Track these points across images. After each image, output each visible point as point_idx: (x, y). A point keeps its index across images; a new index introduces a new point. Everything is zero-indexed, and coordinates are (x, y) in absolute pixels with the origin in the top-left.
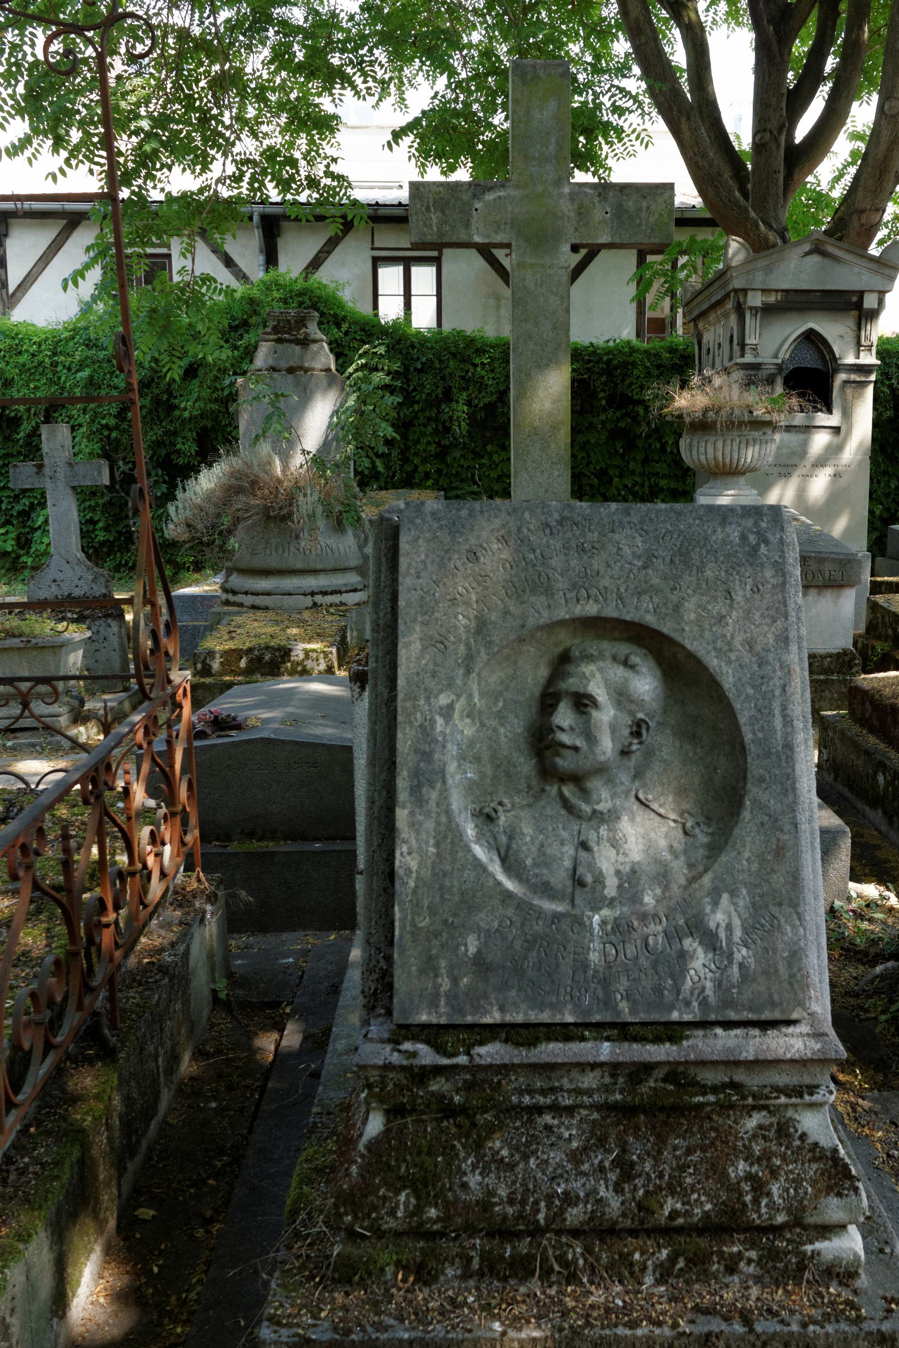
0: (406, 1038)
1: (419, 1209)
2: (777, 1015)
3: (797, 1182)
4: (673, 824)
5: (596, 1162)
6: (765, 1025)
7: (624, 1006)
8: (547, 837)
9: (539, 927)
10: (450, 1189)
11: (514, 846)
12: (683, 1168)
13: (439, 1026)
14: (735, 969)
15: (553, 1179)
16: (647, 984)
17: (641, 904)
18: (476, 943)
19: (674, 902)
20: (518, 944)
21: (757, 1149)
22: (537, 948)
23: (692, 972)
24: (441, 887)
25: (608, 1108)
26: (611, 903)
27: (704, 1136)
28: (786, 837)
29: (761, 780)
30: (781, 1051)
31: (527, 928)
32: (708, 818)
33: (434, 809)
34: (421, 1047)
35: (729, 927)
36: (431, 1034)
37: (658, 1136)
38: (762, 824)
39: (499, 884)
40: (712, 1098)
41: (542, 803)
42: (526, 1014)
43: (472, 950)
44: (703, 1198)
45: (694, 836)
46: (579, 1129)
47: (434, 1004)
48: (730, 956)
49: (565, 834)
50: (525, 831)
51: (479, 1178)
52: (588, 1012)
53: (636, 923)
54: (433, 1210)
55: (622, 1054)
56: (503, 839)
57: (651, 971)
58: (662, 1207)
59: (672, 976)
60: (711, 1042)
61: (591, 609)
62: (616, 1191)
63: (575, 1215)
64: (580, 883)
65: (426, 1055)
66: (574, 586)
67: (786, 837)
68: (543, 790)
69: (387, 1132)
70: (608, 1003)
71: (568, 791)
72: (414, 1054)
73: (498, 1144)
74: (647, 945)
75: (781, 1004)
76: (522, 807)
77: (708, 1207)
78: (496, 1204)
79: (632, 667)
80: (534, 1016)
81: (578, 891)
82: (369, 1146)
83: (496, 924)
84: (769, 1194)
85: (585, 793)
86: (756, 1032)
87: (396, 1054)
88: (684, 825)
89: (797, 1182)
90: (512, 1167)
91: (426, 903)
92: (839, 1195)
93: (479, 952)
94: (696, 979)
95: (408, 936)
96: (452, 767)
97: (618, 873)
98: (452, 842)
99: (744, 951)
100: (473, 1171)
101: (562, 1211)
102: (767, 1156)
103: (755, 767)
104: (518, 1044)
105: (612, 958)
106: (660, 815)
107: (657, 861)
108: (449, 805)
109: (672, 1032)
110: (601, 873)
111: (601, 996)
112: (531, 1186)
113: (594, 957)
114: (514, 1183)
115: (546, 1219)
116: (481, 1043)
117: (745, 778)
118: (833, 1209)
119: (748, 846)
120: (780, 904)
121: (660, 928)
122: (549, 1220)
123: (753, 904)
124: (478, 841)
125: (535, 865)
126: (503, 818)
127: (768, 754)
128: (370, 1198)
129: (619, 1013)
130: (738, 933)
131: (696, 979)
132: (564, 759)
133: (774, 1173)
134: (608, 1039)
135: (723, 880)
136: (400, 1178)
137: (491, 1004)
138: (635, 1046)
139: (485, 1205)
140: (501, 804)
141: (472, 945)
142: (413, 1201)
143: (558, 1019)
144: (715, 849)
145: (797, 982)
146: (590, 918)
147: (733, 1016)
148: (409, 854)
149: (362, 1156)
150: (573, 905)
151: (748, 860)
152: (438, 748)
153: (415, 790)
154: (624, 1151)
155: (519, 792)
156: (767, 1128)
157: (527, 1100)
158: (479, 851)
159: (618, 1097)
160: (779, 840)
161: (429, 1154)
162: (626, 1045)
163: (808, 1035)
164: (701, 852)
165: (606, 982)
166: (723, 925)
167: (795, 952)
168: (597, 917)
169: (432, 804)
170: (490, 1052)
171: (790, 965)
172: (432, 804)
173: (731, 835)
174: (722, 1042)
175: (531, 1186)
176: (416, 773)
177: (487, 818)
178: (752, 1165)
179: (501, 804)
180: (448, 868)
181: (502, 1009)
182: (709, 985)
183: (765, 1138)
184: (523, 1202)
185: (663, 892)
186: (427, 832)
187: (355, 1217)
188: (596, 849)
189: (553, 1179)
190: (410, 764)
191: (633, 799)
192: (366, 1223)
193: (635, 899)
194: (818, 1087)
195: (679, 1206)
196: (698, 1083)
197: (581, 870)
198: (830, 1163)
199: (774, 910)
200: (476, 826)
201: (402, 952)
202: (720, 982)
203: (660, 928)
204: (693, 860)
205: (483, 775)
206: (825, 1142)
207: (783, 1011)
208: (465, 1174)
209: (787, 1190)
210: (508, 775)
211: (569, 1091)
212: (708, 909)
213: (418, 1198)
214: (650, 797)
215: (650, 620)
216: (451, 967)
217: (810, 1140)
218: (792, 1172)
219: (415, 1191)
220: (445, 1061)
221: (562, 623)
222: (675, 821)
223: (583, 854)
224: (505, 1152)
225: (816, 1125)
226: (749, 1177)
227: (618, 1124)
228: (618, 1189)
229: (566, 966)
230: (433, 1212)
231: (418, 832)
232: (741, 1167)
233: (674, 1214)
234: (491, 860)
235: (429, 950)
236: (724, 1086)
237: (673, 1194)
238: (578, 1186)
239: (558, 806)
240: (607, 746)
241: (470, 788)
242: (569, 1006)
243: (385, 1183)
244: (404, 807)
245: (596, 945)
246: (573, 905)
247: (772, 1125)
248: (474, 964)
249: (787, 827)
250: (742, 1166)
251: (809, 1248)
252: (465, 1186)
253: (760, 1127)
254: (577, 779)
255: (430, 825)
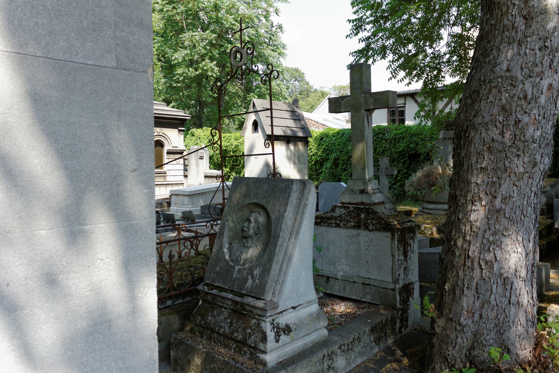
12: (239, 327)
26: (241, 265)
48: (255, 281)
61: (255, 201)
66: (254, 196)
79: (260, 214)
80: (223, 286)
86: (255, 300)
124: (227, 249)
158: (225, 250)
215: (264, 204)
221: (250, 203)
226: (250, 333)
240: (251, 232)
250: (249, 330)
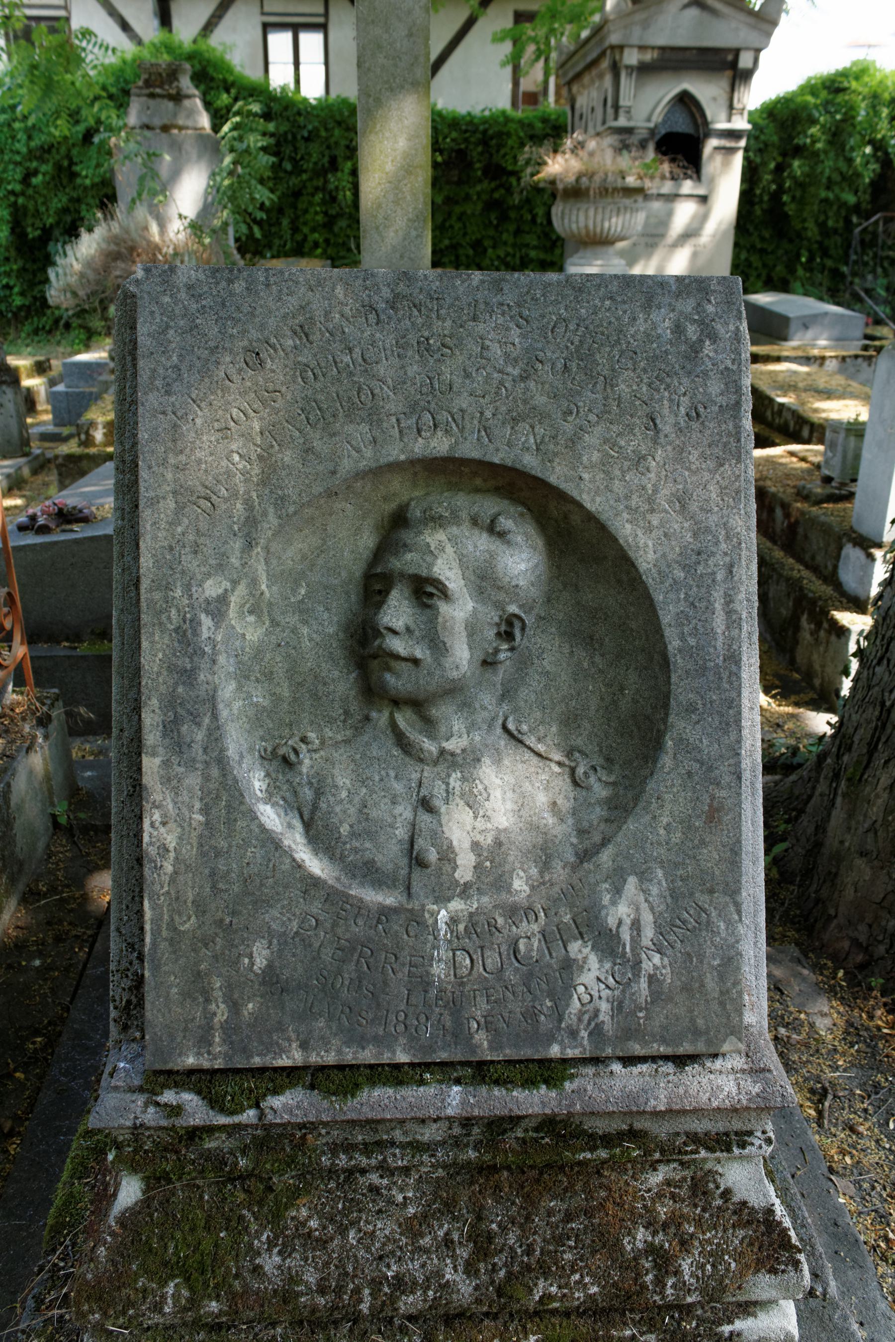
0: (165, 1086)
1: (194, 1303)
2: (701, 1047)
3: (716, 1256)
4: (556, 769)
5: (441, 1233)
6: (681, 1061)
7: (481, 1038)
8: (372, 792)
9: (358, 929)
10: (237, 1276)
11: (323, 806)
12: (559, 1240)
13: (213, 1072)
14: (643, 984)
15: (381, 1258)
16: (516, 1007)
17: (509, 892)
18: (266, 952)
19: (557, 889)
20: (327, 954)
21: (663, 1211)
22: (359, 953)
23: (581, 989)
24: (213, 874)
25: (455, 1169)
26: (465, 891)
27: (590, 1196)
28: (723, 793)
29: (691, 709)
30: (704, 1097)
31: (340, 931)
32: (608, 760)
33: (201, 756)
34: (189, 1098)
35: (636, 925)
36: (201, 1080)
37: (527, 1197)
38: (689, 774)
39: (299, 866)
40: (603, 1154)
41: (366, 738)
42: (339, 1052)
43: (260, 963)
44: (587, 1280)
45: (588, 788)
46: (416, 1190)
47: (204, 1042)
48: (637, 965)
49: (398, 787)
50: (340, 781)
51: (277, 1259)
52: (431, 1048)
53: (500, 921)
54: (214, 1304)
55: (478, 1104)
56: (308, 794)
57: (521, 989)
58: (530, 1291)
59: (551, 995)
60: (605, 1082)
61: (440, 445)
62: (467, 1272)
63: (409, 1302)
64: (418, 861)
65: (194, 1108)
66: (413, 408)
67: (723, 793)
68: (367, 718)
69: (146, 1203)
70: (459, 1034)
71: (403, 719)
72: (176, 1110)
73: (304, 1212)
74: (516, 952)
75: (707, 1032)
76: (336, 744)
77: (594, 1290)
78: (302, 1294)
79: (502, 535)
80: (350, 1056)
81: (417, 874)
82: (122, 1221)
83: (295, 926)
84: (677, 1273)
85: (429, 724)
86: (669, 1068)
87: (151, 1110)
88: (573, 771)
89: (716, 1256)
90: (323, 1243)
91: (190, 896)
92: (773, 1271)
93: (270, 966)
94: (586, 998)
95: (164, 945)
96: (227, 691)
97: (475, 846)
98: (228, 806)
99: (657, 959)
100: (269, 1250)
101: (393, 1299)
102: (674, 1221)
103: (682, 690)
104: (329, 1093)
105: (465, 972)
106: (539, 755)
107: (533, 827)
108: (223, 750)
109: (549, 1072)
110: (450, 846)
111: (448, 1024)
112: (350, 1269)
113: (439, 970)
114: (327, 1264)
115: (370, 1308)
116: (276, 1092)
117: (666, 706)
118: (762, 1285)
119: (668, 806)
120: (711, 891)
121: (535, 927)
122: (375, 1312)
123: (673, 892)
124: (269, 799)
125: (353, 835)
126: (307, 762)
127: (702, 670)
128: (125, 1291)
129: (473, 1049)
130: (648, 933)
131: (586, 998)
132: (398, 676)
133: (685, 1244)
134: (458, 1082)
135: (628, 858)
136: (165, 1264)
137: (289, 1040)
138: (496, 1092)
139: (287, 1296)
140: (304, 740)
141: (260, 956)
142: (185, 1293)
143: (386, 1058)
144: (620, 807)
145: (730, 1001)
146: (434, 914)
147: (638, 1049)
148: (164, 824)
149: (113, 1234)
150: (409, 895)
151: (667, 828)
152: (204, 664)
153: (170, 728)
154: (479, 1218)
155: (331, 721)
156: (678, 1185)
157: (342, 1161)
158: (270, 816)
159: (472, 1154)
160: (712, 798)
161: (207, 1228)
162: (484, 1090)
163: (743, 1071)
164: (599, 812)
165: (456, 1005)
166: (628, 921)
167: (730, 959)
168: (443, 912)
169: (197, 750)
170: (286, 1105)
171: (722, 978)
172: (197, 750)
173: (643, 791)
174: (623, 1081)
175: (350, 1269)
176: (171, 702)
177: (282, 762)
178: (655, 1233)
179: (304, 740)
180: (223, 844)
181: (304, 1046)
182: (604, 1006)
183: (673, 1197)
184: (339, 1290)
185: (541, 873)
186: (190, 790)
187: (105, 1315)
188: (443, 809)
189: (381, 1258)
190: (163, 689)
191: (499, 730)
192: (121, 1320)
193: (501, 883)
194: (750, 1133)
195: (554, 1289)
196: (584, 1132)
197: (420, 843)
198: (762, 1228)
199: (703, 899)
200: (268, 775)
201: (156, 968)
202: (620, 1007)
203: (535, 927)
204: (585, 824)
205: (277, 699)
206: (756, 1201)
207: (709, 1042)
208: (259, 1254)
209: (702, 1267)
210: (315, 696)
211: (403, 1146)
212: (606, 899)
213: (191, 1289)
214: (525, 728)
215: (530, 462)
216: (229, 987)
217: (735, 1199)
218: (709, 1242)
219: (187, 1279)
220: (223, 1120)
221: (394, 467)
222: (559, 764)
223: (425, 818)
224: (313, 1224)
225: (744, 1178)
226: (651, 1249)
227: (472, 1183)
228: (470, 1270)
229: (398, 980)
230: (214, 1306)
231: (176, 791)
232: (640, 1236)
233: (547, 1297)
234: (290, 826)
235: (197, 964)
236: (621, 1136)
237: (546, 1274)
238: (414, 1267)
239: (390, 742)
240: (462, 656)
241: (255, 718)
242: (402, 1040)
243: (145, 1270)
244: (154, 755)
245: (444, 953)
246: (409, 895)
247: (684, 1179)
248: (263, 983)
249: (727, 779)
250: (641, 1234)
251: (726, 1329)
252: (257, 1270)
253: (668, 1183)
254: (418, 705)
255: (193, 780)
